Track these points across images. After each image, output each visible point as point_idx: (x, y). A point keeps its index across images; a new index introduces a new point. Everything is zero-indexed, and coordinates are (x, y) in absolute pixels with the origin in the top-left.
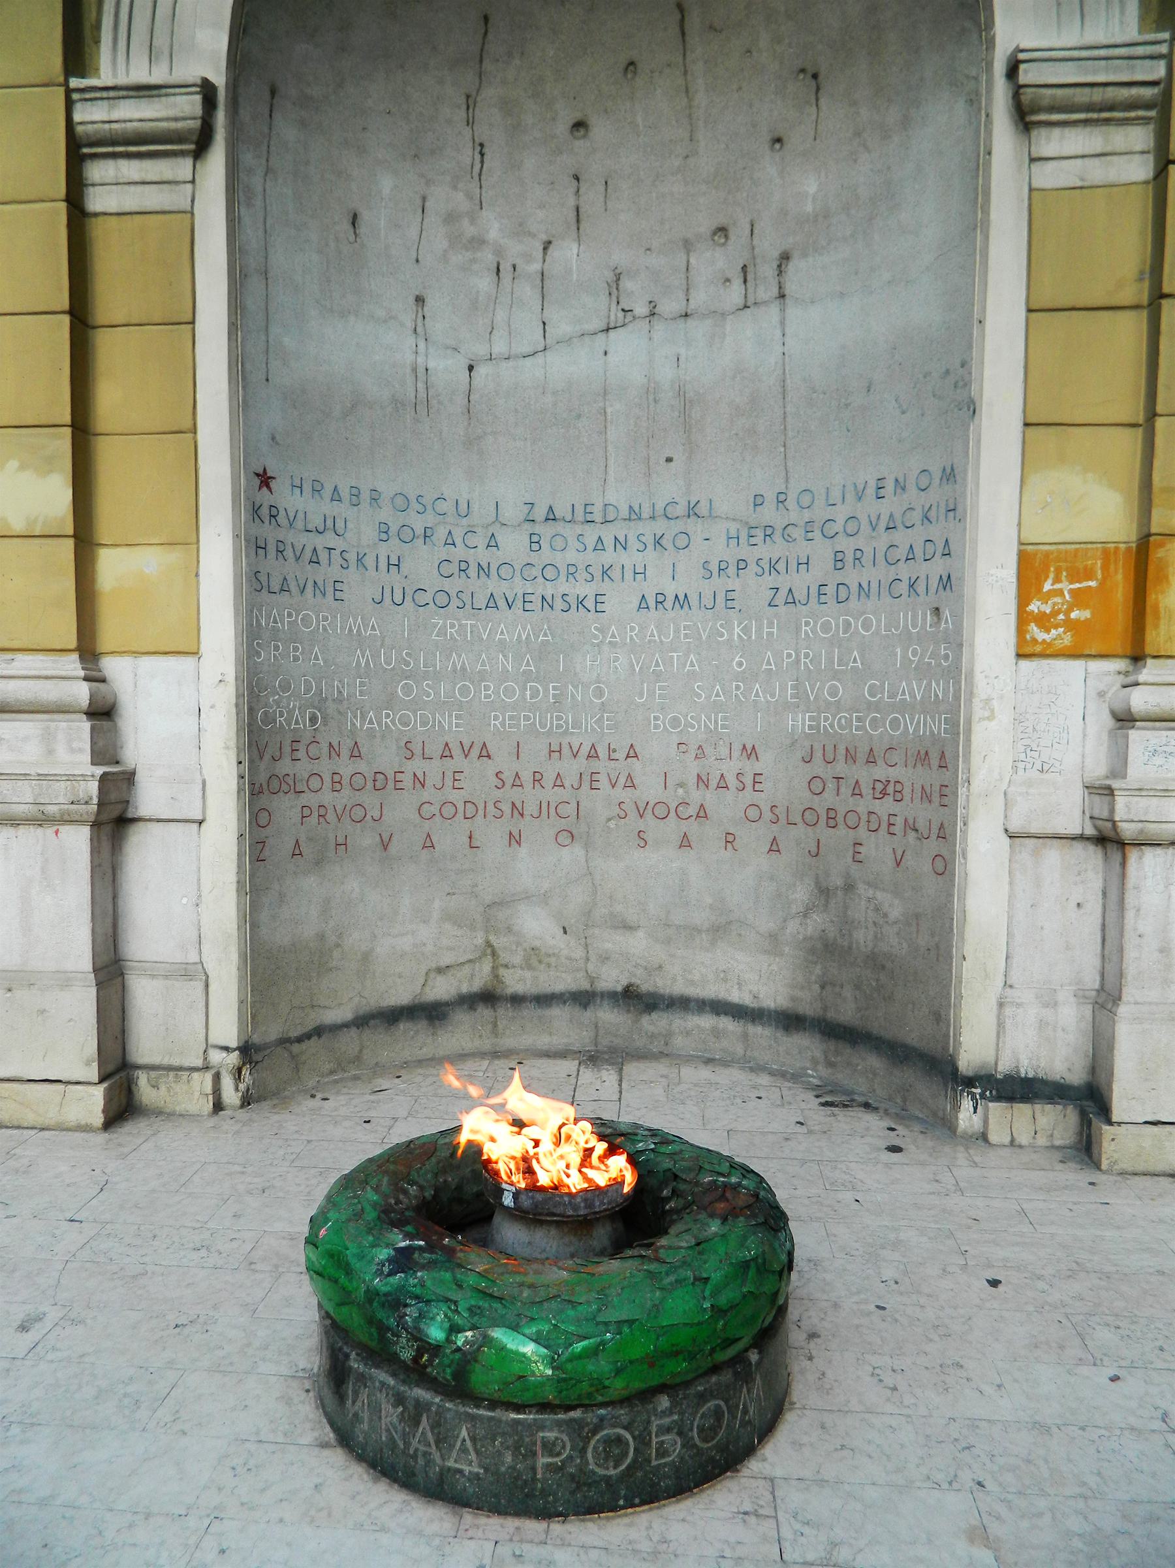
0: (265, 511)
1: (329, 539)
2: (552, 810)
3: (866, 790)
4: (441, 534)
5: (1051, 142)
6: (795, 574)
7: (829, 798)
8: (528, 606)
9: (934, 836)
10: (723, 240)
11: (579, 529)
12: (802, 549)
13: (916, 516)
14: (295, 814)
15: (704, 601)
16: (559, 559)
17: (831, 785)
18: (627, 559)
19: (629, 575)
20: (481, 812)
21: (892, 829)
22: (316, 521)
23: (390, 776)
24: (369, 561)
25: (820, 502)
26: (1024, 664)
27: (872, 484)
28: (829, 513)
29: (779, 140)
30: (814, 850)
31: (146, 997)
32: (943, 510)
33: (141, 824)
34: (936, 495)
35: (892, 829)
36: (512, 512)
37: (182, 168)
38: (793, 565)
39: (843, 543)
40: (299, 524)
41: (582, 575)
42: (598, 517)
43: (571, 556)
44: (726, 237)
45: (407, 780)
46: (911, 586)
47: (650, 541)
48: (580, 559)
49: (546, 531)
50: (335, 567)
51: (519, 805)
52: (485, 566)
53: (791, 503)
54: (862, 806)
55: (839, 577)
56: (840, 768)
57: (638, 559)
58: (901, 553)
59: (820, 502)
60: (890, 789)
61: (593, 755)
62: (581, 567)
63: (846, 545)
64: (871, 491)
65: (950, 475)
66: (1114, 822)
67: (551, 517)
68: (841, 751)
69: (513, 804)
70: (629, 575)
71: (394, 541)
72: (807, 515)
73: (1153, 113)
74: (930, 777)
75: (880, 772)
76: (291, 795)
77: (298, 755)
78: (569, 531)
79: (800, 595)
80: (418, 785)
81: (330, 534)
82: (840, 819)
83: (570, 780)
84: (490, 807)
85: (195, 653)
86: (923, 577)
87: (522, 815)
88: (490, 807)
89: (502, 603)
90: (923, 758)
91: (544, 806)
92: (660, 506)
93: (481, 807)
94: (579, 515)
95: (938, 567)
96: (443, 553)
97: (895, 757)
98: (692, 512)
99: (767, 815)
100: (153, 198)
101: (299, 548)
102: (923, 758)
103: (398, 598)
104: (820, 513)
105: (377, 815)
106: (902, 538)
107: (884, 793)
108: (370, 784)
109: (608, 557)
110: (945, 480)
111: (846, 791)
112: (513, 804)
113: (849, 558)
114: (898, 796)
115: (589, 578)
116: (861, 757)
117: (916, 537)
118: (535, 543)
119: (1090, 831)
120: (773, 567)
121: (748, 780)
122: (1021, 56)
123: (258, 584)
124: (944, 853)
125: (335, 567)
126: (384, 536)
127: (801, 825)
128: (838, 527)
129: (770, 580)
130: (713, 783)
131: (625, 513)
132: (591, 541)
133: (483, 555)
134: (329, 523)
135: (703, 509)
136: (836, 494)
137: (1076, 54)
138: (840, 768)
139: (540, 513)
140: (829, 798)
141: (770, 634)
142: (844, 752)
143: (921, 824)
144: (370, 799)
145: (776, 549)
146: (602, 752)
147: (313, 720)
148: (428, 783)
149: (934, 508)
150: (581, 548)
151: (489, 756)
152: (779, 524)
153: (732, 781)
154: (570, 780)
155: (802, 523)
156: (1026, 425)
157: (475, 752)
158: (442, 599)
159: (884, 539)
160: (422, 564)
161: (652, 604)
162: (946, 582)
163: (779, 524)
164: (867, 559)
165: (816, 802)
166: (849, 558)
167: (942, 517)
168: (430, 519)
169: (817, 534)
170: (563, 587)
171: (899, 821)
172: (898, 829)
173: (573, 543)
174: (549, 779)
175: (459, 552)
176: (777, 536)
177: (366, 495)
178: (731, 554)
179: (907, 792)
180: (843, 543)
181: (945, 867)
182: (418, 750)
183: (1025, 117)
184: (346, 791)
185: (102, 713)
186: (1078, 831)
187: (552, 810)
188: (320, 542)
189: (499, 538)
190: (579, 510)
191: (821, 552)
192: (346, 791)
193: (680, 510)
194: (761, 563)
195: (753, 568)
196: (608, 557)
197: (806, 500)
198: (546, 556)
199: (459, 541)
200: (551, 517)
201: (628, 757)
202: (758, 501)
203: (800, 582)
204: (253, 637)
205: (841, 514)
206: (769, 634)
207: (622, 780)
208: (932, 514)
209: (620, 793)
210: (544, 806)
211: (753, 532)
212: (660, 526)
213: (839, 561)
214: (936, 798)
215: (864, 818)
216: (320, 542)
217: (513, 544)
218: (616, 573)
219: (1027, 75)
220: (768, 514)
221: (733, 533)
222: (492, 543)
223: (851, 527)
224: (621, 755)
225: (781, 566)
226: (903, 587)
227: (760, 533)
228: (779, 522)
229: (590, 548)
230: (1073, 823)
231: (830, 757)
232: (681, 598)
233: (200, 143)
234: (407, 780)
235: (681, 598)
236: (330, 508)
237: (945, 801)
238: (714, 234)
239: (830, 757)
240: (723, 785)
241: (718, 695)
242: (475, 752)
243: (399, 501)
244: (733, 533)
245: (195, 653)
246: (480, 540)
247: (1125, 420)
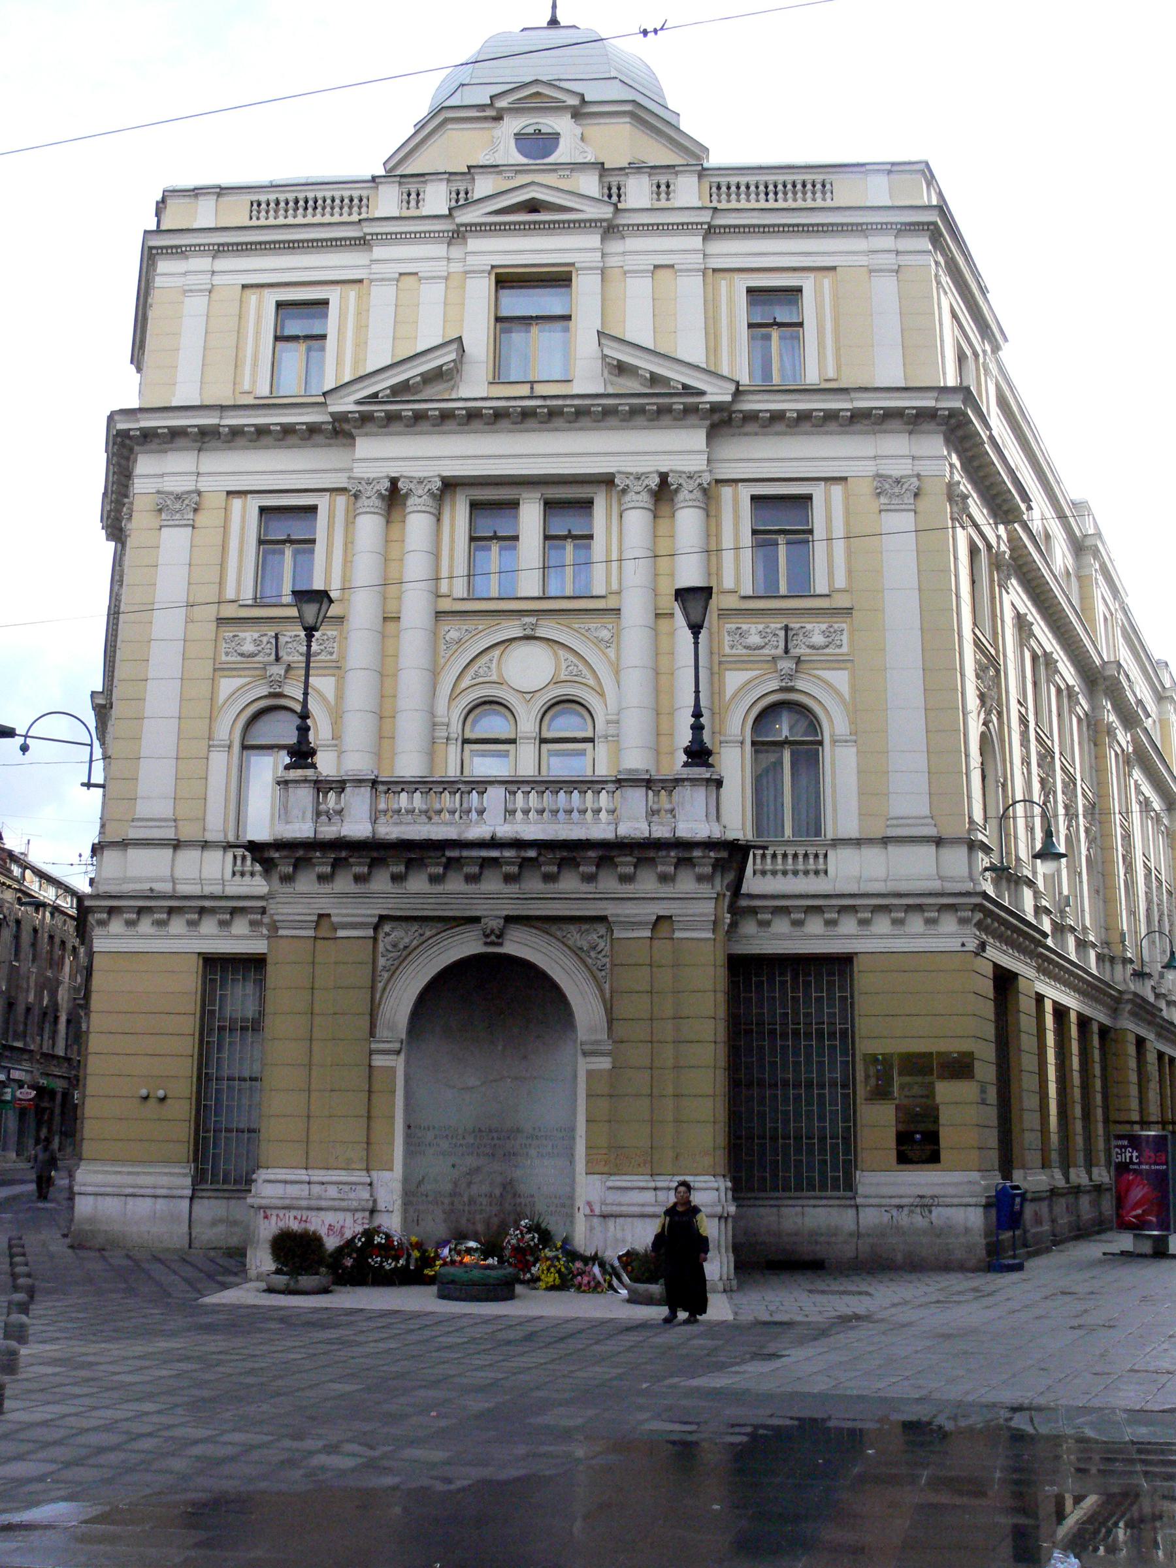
5: (589, 1059)
12: (545, 1142)
37: (394, 1057)
83: (484, 1203)
100: (388, 1064)
123: (409, 1153)
154: (484, 1203)
160: (445, 1145)
175: (454, 1141)
178: (529, 1141)
181: (572, 1222)
185: (371, 1184)
196: (496, 1141)
200: (480, 1130)
204: (405, 1165)
222: (464, 1138)
233: (398, 1053)
246: (460, 1137)
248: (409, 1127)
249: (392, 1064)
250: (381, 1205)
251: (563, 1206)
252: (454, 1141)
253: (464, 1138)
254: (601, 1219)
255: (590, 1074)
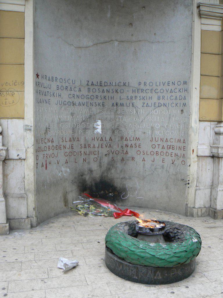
0: (37, 83)
1: (48, 90)
2: (93, 153)
3: (166, 147)
4: (69, 88)
6: (148, 100)
7: (156, 149)
8: (87, 105)
9: (182, 157)
10: (131, 26)
11: (99, 87)
12: (150, 95)
13: (177, 90)
14: (42, 156)
15: (127, 105)
16: (94, 94)
17: (157, 146)
18: (110, 95)
19: (110, 98)
20: (77, 154)
21: (172, 155)
22: (45, 85)
23: (59, 146)
24: (55, 94)
25: (154, 85)
26: (201, 122)
27: (167, 82)
28: (156, 88)
29: (144, 7)
30: (153, 161)
31: (13, 203)
32: (184, 90)
33: (12, 161)
34: (181, 87)
35: (172, 155)
36: (84, 83)
38: (148, 98)
39: (159, 94)
40: (43, 86)
41: (99, 98)
42: (103, 85)
43: (97, 93)
44: (132, 25)
45: (62, 147)
46: (176, 105)
47: (114, 90)
48: (99, 94)
49: (92, 88)
50: (49, 96)
51: (85, 152)
52: (78, 95)
53: (147, 84)
54: (165, 151)
55: (159, 101)
56: (159, 142)
57: (112, 95)
58: (174, 98)
59: (154, 85)
60: (171, 147)
61: (102, 140)
62: (99, 96)
63: (161, 95)
64: (166, 84)
65: (185, 83)
66: (218, 154)
67: (92, 84)
68: (159, 139)
69: (84, 152)
70: (110, 98)
71: (60, 90)
72: (151, 88)
73: (221, 19)
74: (181, 145)
75: (169, 143)
76: (42, 152)
77: (43, 142)
78: (96, 88)
79: (150, 105)
80: (64, 148)
81: (48, 88)
82: (159, 154)
83: (97, 145)
84: (79, 153)
85: (23, 118)
86: (179, 103)
87: (86, 154)
88: (79, 153)
89: (82, 105)
90: (179, 141)
91: (91, 152)
92: (117, 84)
93: (77, 153)
94: (99, 84)
95: (183, 101)
96: (69, 92)
97: (172, 140)
98: (124, 85)
99: (142, 153)
101: (43, 92)
102: (179, 141)
103: (60, 103)
104: (155, 87)
105: (56, 156)
106: (173, 94)
107: (170, 148)
108: (55, 148)
109: (105, 94)
110: (184, 84)
111: (161, 147)
112: (84, 152)
113: (161, 97)
114: (173, 149)
115: (101, 99)
116: (165, 140)
117: (178, 94)
118: (89, 89)
119: (211, 155)
120: (143, 98)
121: (138, 145)
122: (201, 5)
124: (184, 160)
125: (49, 96)
126: (58, 88)
127: (150, 155)
128: (159, 91)
129: (142, 101)
130: (129, 146)
131: (109, 84)
132: (101, 90)
133: (77, 93)
134: (48, 86)
135: (127, 84)
136: (158, 84)
137: (209, 6)
138: (159, 142)
139: (90, 83)
140: (156, 149)
141: (142, 113)
142: (160, 139)
143: (179, 155)
144: (55, 152)
145: (144, 95)
146: (104, 139)
147: (45, 133)
148: (67, 148)
149: (182, 89)
150: (99, 92)
151: (79, 141)
152: (145, 89)
153: (134, 145)
154: (97, 145)
155: (150, 89)
156: (201, 75)
157: (76, 140)
158: (69, 104)
159: (169, 95)
160: (65, 96)
161: (115, 105)
162: (185, 105)
163: (145, 89)
164: (166, 98)
165: (153, 150)
166: (161, 97)
167: (184, 91)
168: (67, 84)
169: (154, 92)
170: (95, 100)
171: (173, 154)
172: (173, 155)
173: (97, 90)
174: (92, 146)
175: (73, 92)
176: (144, 91)
177: (54, 79)
179: (175, 148)
180: (159, 94)
182: (64, 140)
183: (200, 15)
184: (51, 150)
186: (209, 155)
187: (93, 153)
188: (47, 90)
189: (81, 89)
190: (99, 83)
191: (155, 97)
192: (51, 150)
193: (122, 84)
194: (141, 97)
195: (138, 98)
197: (151, 84)
198: (91, 93)
199: (73, 90)
200: (92, 84)
201: (110, 140)
202: (140, 84)
203: (150, 102)
204: (36, 113)
205: (159, 88)
206: (142, 113)
207: (108, 145)
208: (181, 91)
209: (108, 149)
210: (91, 152)
211: (138, 90)
212: (117, 87)
213: (159, 98)
214: (182, 149)
215: (165, 153)
216: (47, 90)
217: (84, 92)
218: (107, 98)
219: (202, 8)
220: (142, 86)
221: (134, 90)
222: (80, 90)
223: (162, 91)
224: (108, 140)
225: (145, 98)
226: (174, 105)
227: (140, 91)
228: (145, 88)
229: (101, 92)
230: (207, 153)
231: (157, 140)
232: (122, 104)
234: (62, 147)
235: (122, 104)
236: (48, 82)
237: (185, 149)
238: (129, 24)
239: (157, 140)
240: (132, 146)
241: (130, 126)
242: (76, 140)
243: (61, 80)
244: (134, 90)
245: (23, 118)
246: (77, 89)
247: (216, 75)
248: (38, 76)
249: (20, 9)
250: (13, 154)
251: (169, 147)
252: (73, 92)
253: (80, 90)
254: (210, 160)
255: (202, 31)
